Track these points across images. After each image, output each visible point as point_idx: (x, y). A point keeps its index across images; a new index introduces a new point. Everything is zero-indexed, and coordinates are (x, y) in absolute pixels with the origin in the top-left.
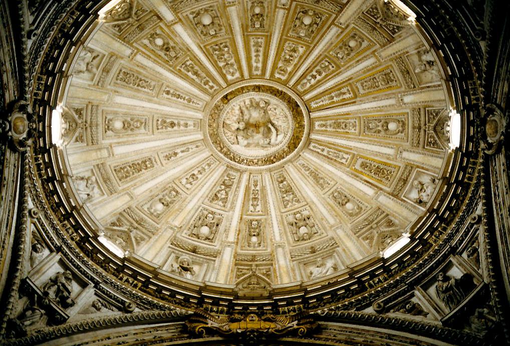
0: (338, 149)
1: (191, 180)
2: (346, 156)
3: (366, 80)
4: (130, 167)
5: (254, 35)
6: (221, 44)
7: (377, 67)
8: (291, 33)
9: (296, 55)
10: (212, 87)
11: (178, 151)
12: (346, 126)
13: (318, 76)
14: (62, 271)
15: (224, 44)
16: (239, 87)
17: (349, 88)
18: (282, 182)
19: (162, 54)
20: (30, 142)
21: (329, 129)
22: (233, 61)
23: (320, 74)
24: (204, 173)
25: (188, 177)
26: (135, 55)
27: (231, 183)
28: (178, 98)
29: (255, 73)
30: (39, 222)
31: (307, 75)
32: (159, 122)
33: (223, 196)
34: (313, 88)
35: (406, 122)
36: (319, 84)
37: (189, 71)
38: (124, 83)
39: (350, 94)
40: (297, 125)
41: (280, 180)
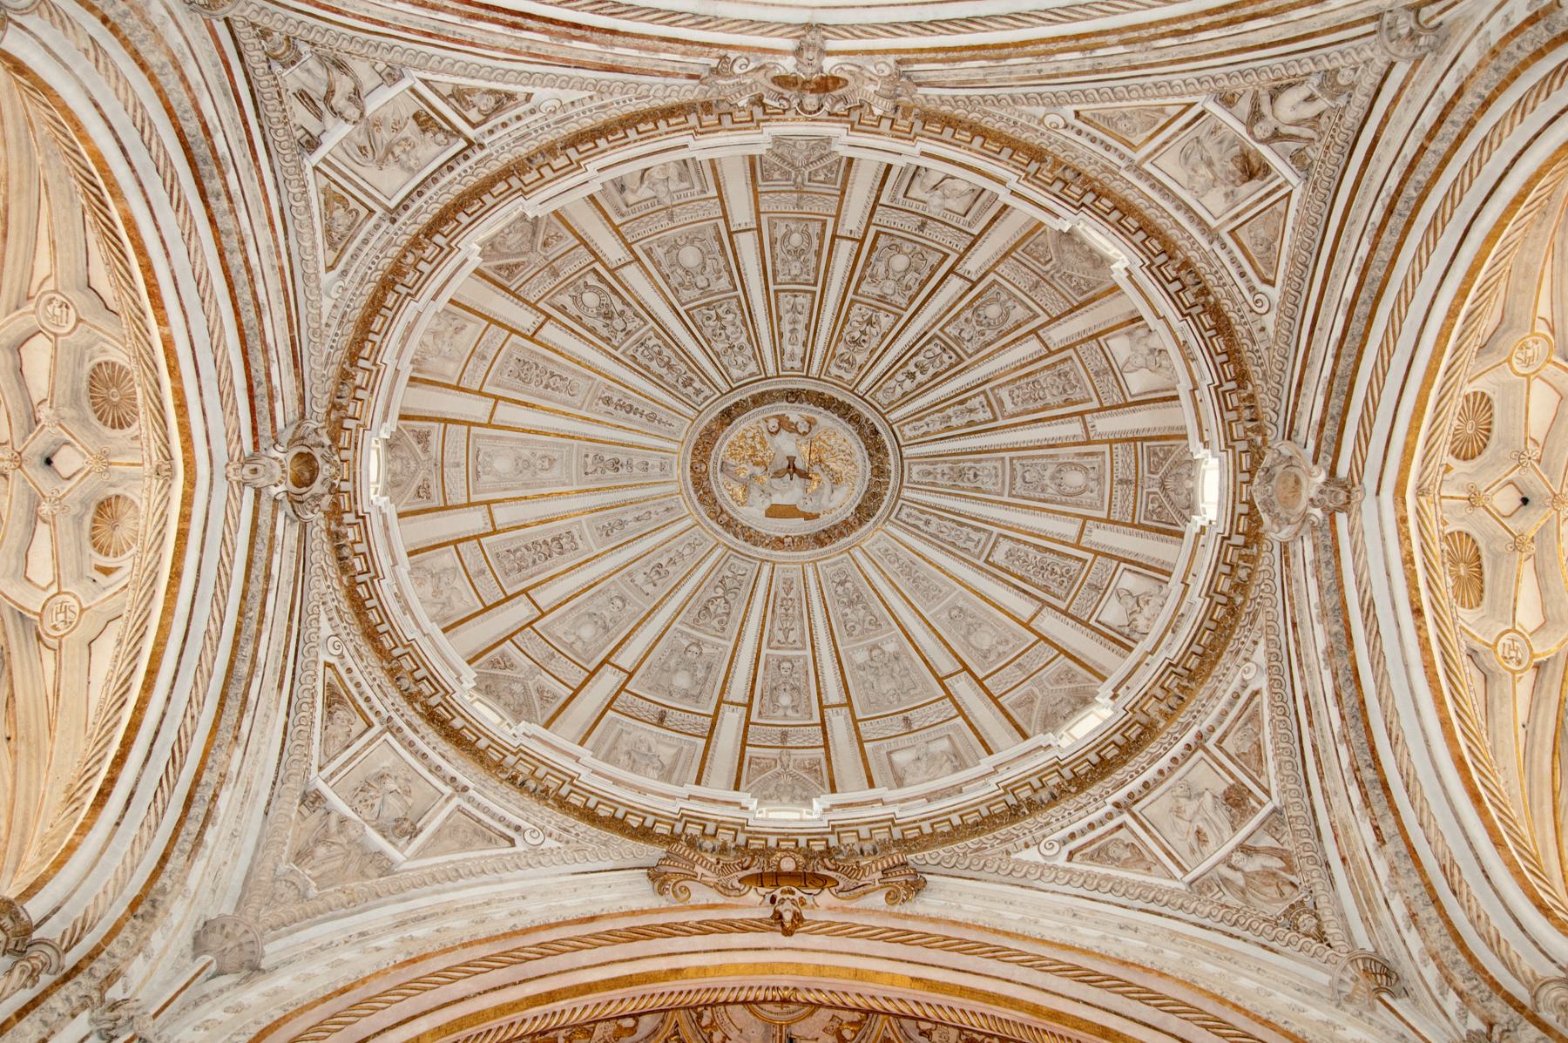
2: (975, 536)
8: (864, 287)
9: (874, 331)
10: (698, 392)
11: (629, 517)
12: (976, 475)
13: (918, 374)
15: (725, 306)
16: (755, 392)
17: (982, 398)
18: (842, 583)
19: (599, 324)
20: (327, 500)
22: (743, 339)
26: (540, 327)
27: (736, 584)
28: (628, 412)
29: (788, 364)
32: (589, 460)
33: (720, 611)
34: (907, 398)
36: (921, 390)
37: (651, 360)
40: (876, 471)
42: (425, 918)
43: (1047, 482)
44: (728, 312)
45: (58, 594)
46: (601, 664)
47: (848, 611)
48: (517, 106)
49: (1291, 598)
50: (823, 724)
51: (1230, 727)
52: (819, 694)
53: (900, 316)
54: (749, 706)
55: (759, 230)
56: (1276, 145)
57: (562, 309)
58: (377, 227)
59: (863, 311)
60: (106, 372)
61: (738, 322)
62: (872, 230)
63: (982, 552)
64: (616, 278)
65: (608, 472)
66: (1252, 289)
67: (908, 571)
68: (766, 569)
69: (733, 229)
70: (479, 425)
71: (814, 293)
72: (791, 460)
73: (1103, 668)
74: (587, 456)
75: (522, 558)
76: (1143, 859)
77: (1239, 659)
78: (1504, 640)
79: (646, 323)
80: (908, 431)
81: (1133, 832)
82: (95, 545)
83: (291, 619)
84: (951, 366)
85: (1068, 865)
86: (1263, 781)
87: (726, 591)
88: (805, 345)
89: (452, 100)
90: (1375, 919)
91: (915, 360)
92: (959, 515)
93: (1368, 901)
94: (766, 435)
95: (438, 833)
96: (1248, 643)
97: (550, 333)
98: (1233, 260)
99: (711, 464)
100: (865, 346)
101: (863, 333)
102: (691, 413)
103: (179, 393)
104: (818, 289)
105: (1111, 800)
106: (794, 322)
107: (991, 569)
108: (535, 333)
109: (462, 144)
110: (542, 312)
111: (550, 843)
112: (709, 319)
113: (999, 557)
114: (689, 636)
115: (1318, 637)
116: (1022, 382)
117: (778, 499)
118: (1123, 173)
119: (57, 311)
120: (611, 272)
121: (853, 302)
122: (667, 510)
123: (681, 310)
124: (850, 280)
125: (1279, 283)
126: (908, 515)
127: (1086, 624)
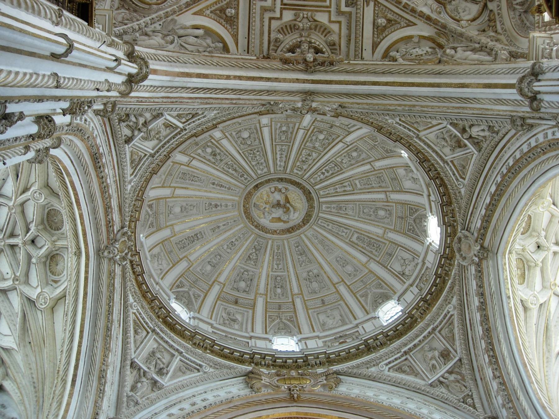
0: (340, 225)
1: (230, 246)
4: (186, 239)
7: (371, 172)
8: (308, 144)
10: (246, 179)
11: (221, 225)
12: (346, 209)
14: (155, 346)
18: (297, 247)
19: (211, 158)
21: (333, 210)
22: (263, 161)
23: (328, 172)
24: (239, 241)
25: (228, 244)
27: (259, 248)
29: (279, 169)
30: (138, 312)
32: (207, 205)
33: (254, 258)
34: (322, 181)
36: (327, 179)
37: (229, 168)
38: (182, 180)
42: (175, 404)
43: (372, 213)
44: (258, 151)
45: (42, 292)
46: (214, 282)
47: (300, 257)
48: (199, 115)
49: (465, 284)
50: (293, 301)
51: (444, 326)
52: (291, 289)
54: (266, 295)
56: (470, 140)
57: (199, 155)
58: (147, 159)
60: (53, 212)
62: (313, 127)
63: (348, 237)
64: (219, 144)
66: (457, 180)
67: (322, 242)
68: (270, 242)
70: (169, 198)
71: (289, 145)
72: (278, 201)
73: (393, 286)
75: (184, 243)
76: (414, 372)
77: (447, 303)
78: (531, 297)
79: (228, 157)
80: (321, 193)
81: (410, 362)
82: (51, 272)
83: (121, 300)
84: (338, 171)
85: (388, 373)
86: (454, 347)
88: (285, 162)
90: (491, 401)
93: (489, 395)
94: (270, 193)
95: (174, 371)
96: (450, 297)
97: (194, 163)
98: (451, 169)
101: (306, 158)
102: (243, 186)
103: (84, 231)
104: (291, 144)
105: (403, 351)
106: (282, 154)
107: (352, 244)
109: (179, 130)
110: (192, 157)
111: (212, 370)
113: (354, 239)
114: (243, 268)
115: (476, 302)
116: (364, 179)
117: (274, 215)
119: (38, 196)
120: (217, 142)
121: (303, 149)
122: (234, 221)
123: (241, 152)
124: (303, 142)
125: (467, 179)
126: (321, 222)
127: (387, 268)
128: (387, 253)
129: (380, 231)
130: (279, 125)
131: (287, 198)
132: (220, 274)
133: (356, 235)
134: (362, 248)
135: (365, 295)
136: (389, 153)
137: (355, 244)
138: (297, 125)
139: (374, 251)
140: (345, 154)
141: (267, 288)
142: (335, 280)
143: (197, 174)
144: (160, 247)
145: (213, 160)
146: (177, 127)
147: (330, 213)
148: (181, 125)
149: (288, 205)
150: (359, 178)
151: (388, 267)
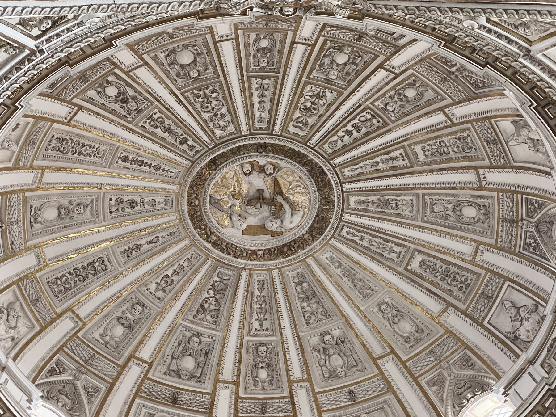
3: (429, 143)
5: (258, 76)
6: (207, 88)
7: (446, 127)
8: (314, 73)
9: (321, 102)
10: (191, 148)
12: (397, 205)
19: (117, 107)
22: (224, 110)
23: (358, 129)
28: (141, 166)
29: (257, 125)
31: (338, 131)
32: (113, 203)
33: (212, 307)
34: (346, 148)
35: (491, 210)
36: (356, 143)
37: (156, 127)
39: (404, 160)
40: (323, 202)
41: (297, 281)
44: (213, 91)
46: (128, 360)
47: (305, 304)
52: (287, 371)
53: (342, 93)
54: (237, 383)
55: (237, 39)
57: (91, 101)
59: (314, 88)
61: (221, 98)
62: (322, 39)
64: (130, 77)
65: (127, 210)
67: (349, 274)
68: (244, 274)
69: (217, 40)
70: (31, 190)
73: (495, 363)
74: (111, 200)
84: (379, 128)
87: (216, 292)
88: (270, 112)
89: (19, 26)
91: (352, 123)
92: (385, 234)
94: (242, 176)
99: (201, 199)
100: (315, 112)
104: (281, 75)
106: (262, 96)
108: (70, 120)
109: (27, 52)
112: (198, 97)
116: (432, 142)
118: (521, 60)
120: (127, 73)
123: (178, 93)
124: (304, 69)
126: (348, 233)
128: (482, 294)
129: (466, 249)
130: (253, 36)
131: (276, 184)
132: (141, 342)
133: (419, 258)
134: (432, 283)
135: (438, 382)
136: (480, 88)
137: (416, 275)
138: (290, 34)
139: (456, 291)
140: (392, 93)
141: (239, 369)
142: (377, 349)
143: (89, 139)
144: (14, 292)
145: (123, 112)
146: (21, 47)
147: (365, 213)
148: (31, 44)
149: (279, 199)
150: (421, 142)
151: (485, 323)
